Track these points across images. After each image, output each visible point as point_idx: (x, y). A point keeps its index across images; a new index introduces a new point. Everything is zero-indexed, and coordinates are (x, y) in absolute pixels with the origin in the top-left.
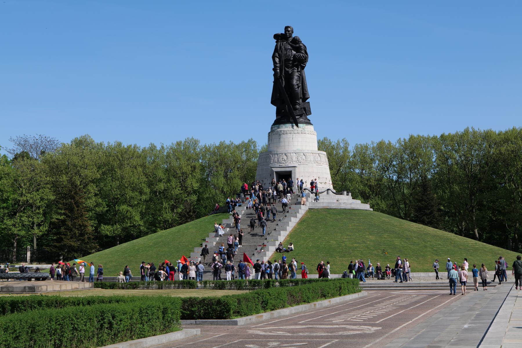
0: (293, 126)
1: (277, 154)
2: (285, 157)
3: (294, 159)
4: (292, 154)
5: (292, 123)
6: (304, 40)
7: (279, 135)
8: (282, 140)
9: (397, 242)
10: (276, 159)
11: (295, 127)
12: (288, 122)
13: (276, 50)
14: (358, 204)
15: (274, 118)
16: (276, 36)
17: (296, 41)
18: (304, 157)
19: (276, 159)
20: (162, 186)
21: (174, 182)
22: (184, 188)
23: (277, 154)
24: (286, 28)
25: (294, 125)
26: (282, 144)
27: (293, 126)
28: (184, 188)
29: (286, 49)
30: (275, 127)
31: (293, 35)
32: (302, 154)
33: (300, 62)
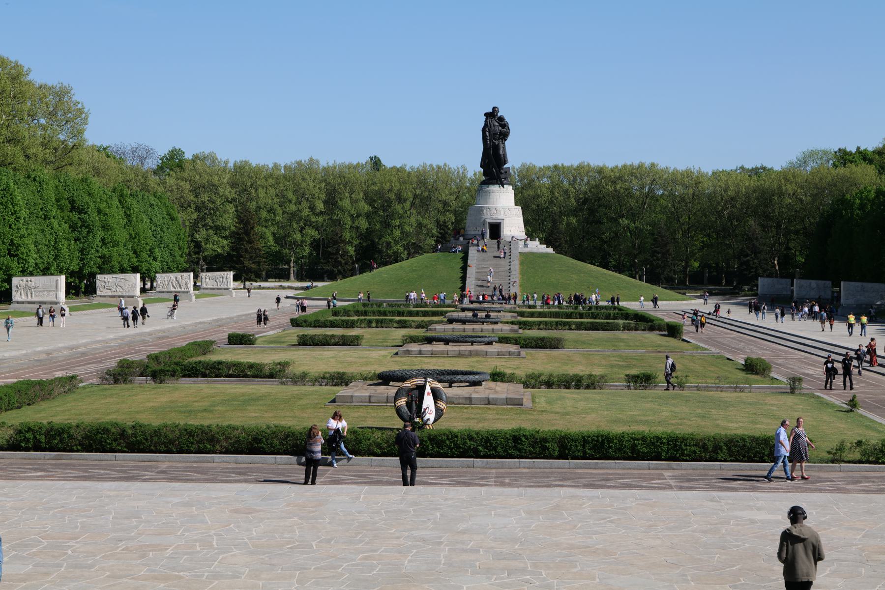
6: (508, 119)
7: (488, 192)
9: (592, 280)
12: (497, 183)
13: (486, 126)
14: (543, 249)
16: (486, 114)
17: (501, 119)
20: (293, 208)
21: (305, 205)
22: (312, 208)
24: (494, 108)
28: (312, 208)
29: (494, 126)
30: (484, 187)
31: (499, 115)
33: (504, 136)
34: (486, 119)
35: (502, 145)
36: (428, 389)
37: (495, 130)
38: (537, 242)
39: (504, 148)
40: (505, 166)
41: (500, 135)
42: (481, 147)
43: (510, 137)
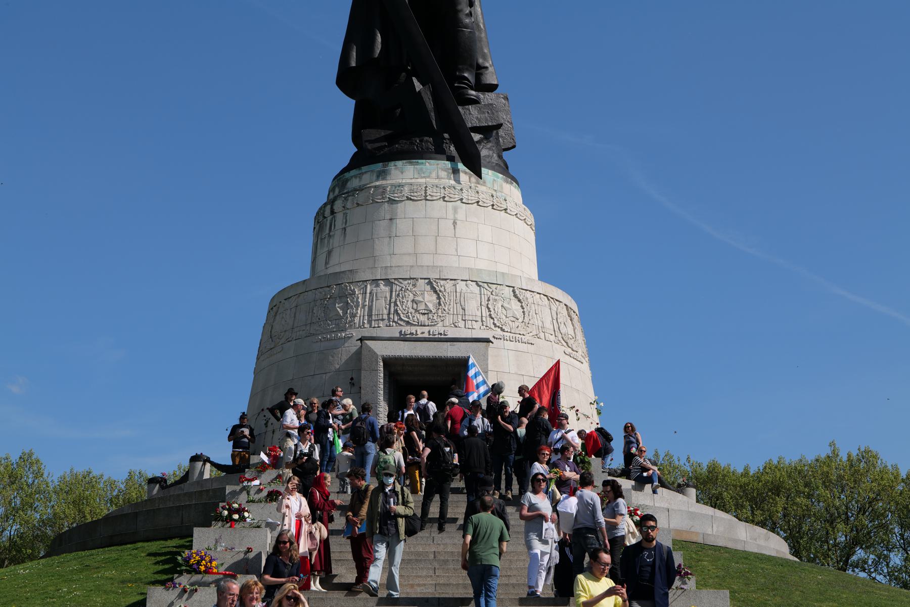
0: (456, 171)
1: (388, 282)
2: (430, 299)
3: (473, 307)
4: (461, 286)
5: (451, 159)
8: (402, 225)
10: (381, 306)
11: (466, 175)
18: (515, 306)
19: (381, 306)
23: (388, 282)
25: (461, 166)
26: (403, 246)
27: (456, 171)
32: (508, 292)
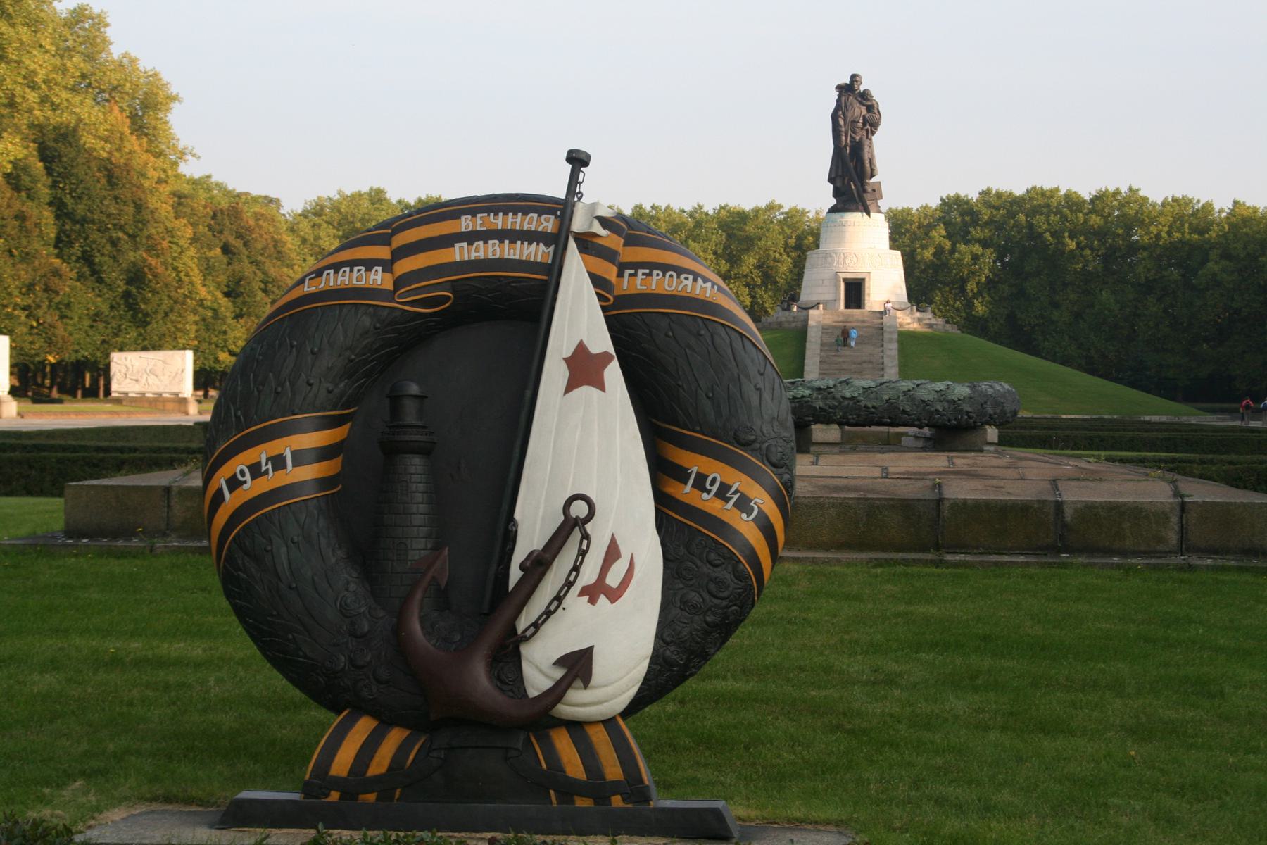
6: (877, 96)
15: (833, 201)
16: (839, 88)
17: (865, 97)
24: (854, 77)
30: (836, 216)
31: (862, 89)
33: (872, 124)
34: (840, 96)
35: (867, 142)
36: (578, 319)
37: (854, 115)
38: (929, 315)
39: (870, 146)
40: (873, 180)
41: (864, 124)
42: (832, 147)
43: (880, 128)
